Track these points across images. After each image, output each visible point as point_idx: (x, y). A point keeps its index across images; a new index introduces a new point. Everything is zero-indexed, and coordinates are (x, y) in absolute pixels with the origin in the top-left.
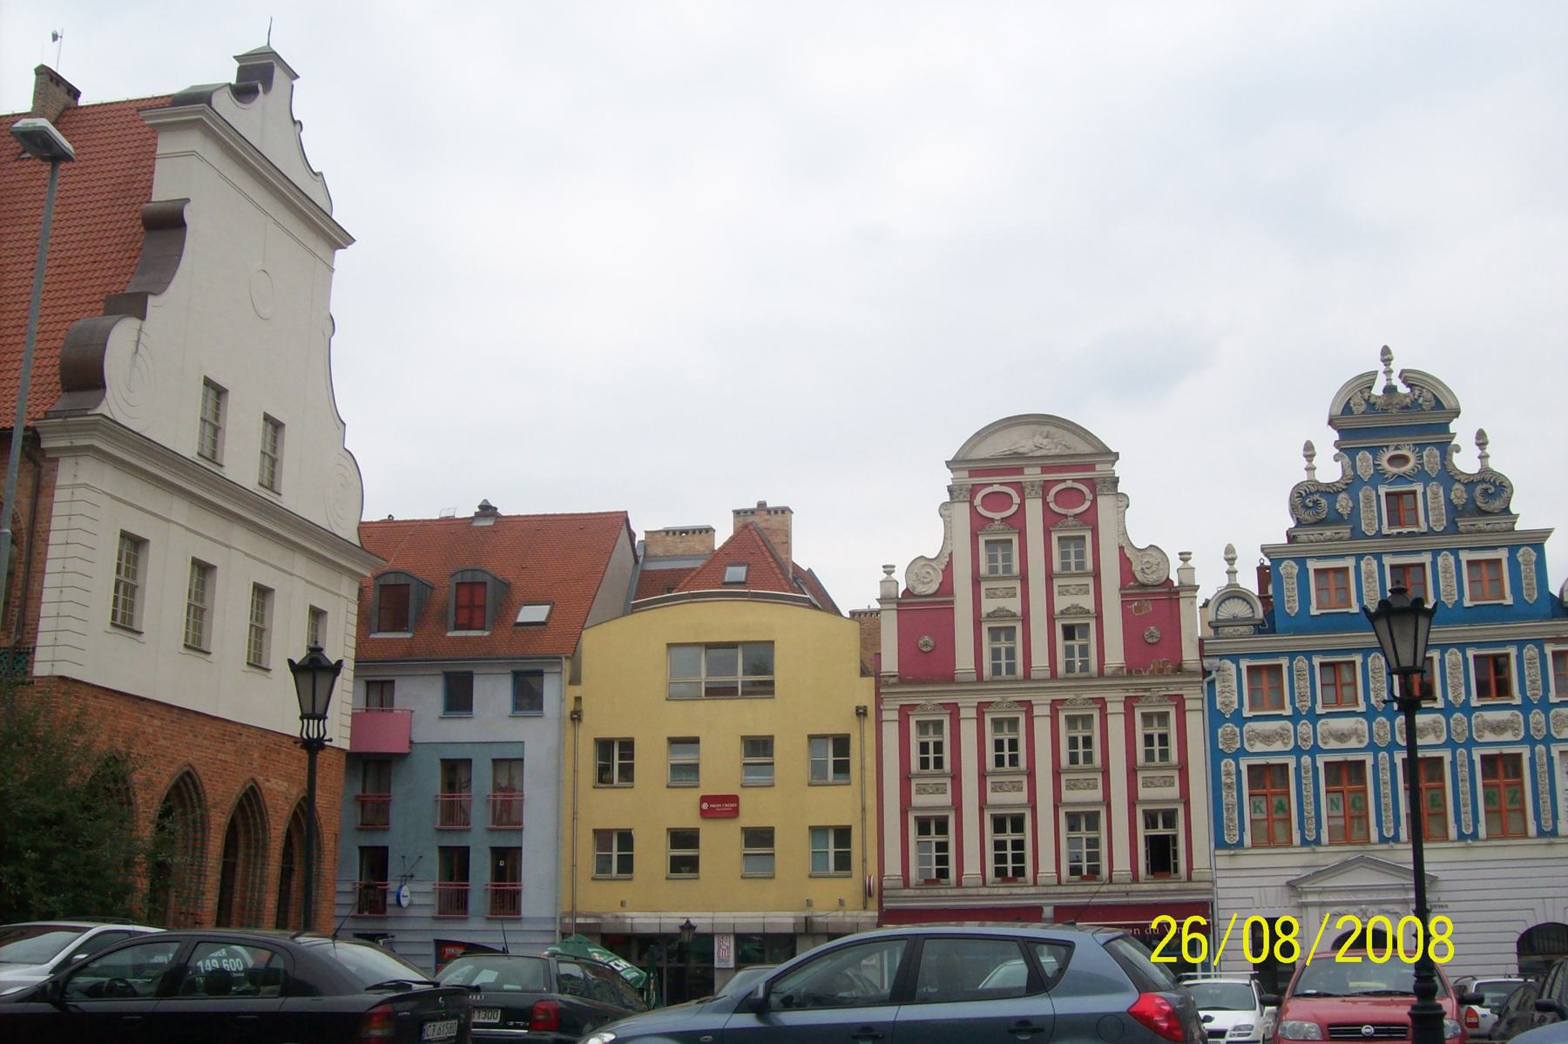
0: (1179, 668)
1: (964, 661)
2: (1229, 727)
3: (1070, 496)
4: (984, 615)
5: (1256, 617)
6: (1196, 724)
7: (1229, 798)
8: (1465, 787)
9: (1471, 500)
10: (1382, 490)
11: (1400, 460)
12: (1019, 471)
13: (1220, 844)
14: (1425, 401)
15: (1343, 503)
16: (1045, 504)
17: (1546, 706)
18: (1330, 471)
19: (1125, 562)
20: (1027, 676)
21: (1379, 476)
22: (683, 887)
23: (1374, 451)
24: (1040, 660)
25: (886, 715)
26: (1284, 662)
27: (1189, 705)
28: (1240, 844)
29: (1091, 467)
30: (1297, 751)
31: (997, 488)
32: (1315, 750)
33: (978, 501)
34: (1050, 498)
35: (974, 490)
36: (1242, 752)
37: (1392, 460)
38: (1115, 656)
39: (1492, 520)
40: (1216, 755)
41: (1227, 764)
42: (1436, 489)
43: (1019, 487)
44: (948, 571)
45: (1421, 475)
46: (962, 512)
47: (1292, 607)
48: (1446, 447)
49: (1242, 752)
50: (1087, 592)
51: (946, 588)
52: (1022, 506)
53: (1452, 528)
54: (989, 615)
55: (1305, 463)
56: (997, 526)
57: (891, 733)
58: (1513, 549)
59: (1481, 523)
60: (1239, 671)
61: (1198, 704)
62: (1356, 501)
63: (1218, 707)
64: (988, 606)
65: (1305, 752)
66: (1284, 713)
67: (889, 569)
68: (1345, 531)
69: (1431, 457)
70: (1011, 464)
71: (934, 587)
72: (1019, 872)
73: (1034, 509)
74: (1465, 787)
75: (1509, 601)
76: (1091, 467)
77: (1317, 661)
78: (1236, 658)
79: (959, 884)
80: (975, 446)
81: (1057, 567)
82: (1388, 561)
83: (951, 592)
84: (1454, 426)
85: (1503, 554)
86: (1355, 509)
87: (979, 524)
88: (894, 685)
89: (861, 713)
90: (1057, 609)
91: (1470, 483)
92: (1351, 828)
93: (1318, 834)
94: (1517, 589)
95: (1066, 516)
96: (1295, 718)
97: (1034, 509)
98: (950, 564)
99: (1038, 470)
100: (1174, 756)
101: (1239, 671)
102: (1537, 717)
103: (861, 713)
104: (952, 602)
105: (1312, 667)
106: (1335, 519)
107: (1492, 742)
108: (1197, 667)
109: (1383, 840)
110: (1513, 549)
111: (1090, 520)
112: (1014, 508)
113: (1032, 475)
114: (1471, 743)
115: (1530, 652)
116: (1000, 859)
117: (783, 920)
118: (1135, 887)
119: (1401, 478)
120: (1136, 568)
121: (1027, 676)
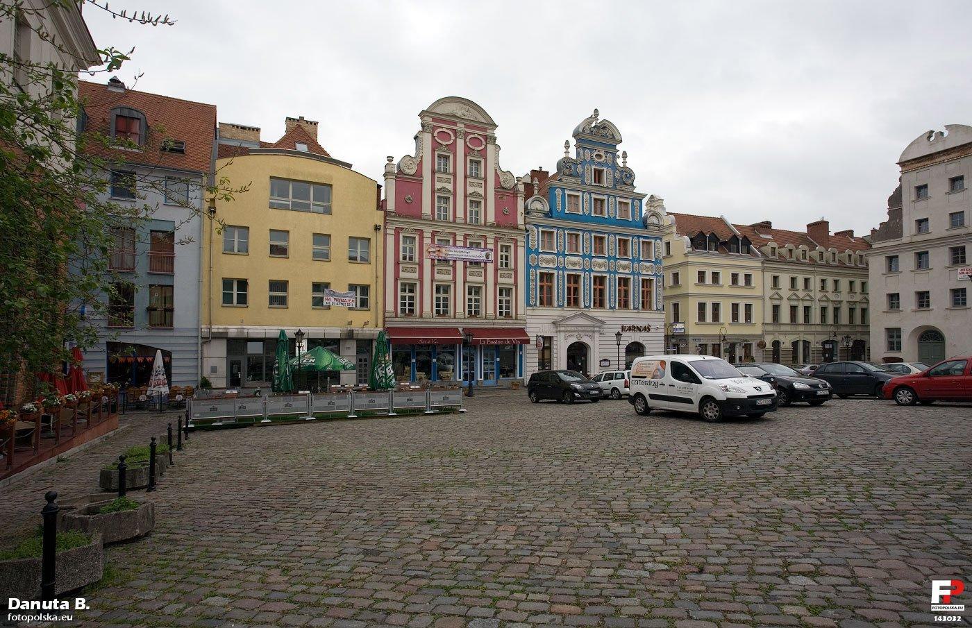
0: (516, 228)
1: (426, 209)
2: (532, 256)
4: (436, 189)
5: (545, 210)
6: (521, 252)
7: (532, 285)
8: (613, 289)
10: (593, 167)
11: (600, 156)
12: (455, 124)
13: (528, 305)
15: (579, 169)
16: (465, 142)
18: (573, 154)
19: (497, 175)
20: (454, 221)
22: (278, 312)
23: (592, 150)
24: (460, 214)
25: (388, 231)
26: (555, 231)
27: (519, 244)
28: (535, 305)
29: (485, 130)
30: (558, 268)
31: (444, 130)
32: (564, 269)
33: (435, 134)
34: (468, 140)
35: (435, 127)
36: (538, 266)
37: (596, 155)
38: (491, 218)
39: (628, 187)
40: (528, 267)
43: (455, 132)
44: (420, 164)
45: (605, 164)
46: (427, 138)
47: (559, 208)
48: (615, 156)
49: (538, 266)
50: (481, 187)
51: (419, 173)
52: (455, 141)
53: (614, 187)
54: (438, 190)
55: (565, 150)
56: (443, 148)
57: (391, 240)
59: (624, 187)
60: (538, 232)
61: (522, 244)
62: (584, 169)
63: (530, 246)
64: (438, 185)
65: (561, 269)
66: (554, 252)
67: (390, 159)
68: (580, 181)
70: (451, 119)
71: (412, 172)
72: (445, 312)
73: (460, 143)
74: (613, 289)
76: (485, 130)
77: (566, 232)
78: (537, 226)
79: (421, 316)
80: (434, 108)
81: (468, 174)
82: (593, 196)
83: (421, 176)
84: (618, 147)
86: (583, 172)
87: (436, 146)
88: (394, 216)
89: (377, 228)
90: (468, 193)
92: (573, 301)
93: (590, 304)
94: (633, 216)
95: (474, 150)
96: (558, 255)
97: (460, 143)
98: (421, 162)
99: (463, 126)
100: (512, 265)
101: (538, 232)
102: (636, 265)
103: (377, 228)
104: (422, 180)
105: (565, 234)
107: (623, 273)
108: (523, 227)
109: (585, 307)
111: (483, 153)
112: (452, 141)
113: (460, 127)
114: (616, 272)
115: (636, 240)
116: (403, 305)
117: (335, 332)
118: (496, 321)
119: (599, 163)
120: (501, 180)
121: (454, 221)
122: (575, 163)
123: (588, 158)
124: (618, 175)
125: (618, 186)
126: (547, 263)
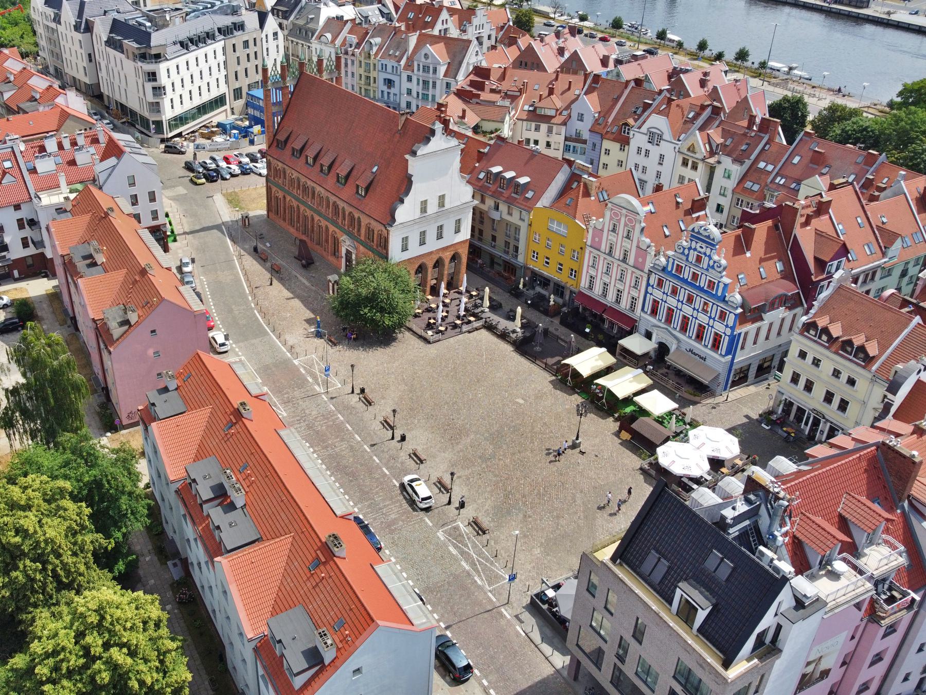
3: (630, 221)
9: (713, 266)
11: (701, 247)
14: (712, 238)
17: (714, 319)
21: (695, 249)
23: (697, 242)
36: (651, 294)
40: (646, 292)
41: (648, 295)
42: (707, 259)
47: (669, 269)
51: (602, 230)
53: (707, 270)
58: (719, 282)
69: (708, 250)
75: (714, 293)
85: (716, 282)
91: (715, 262)
103: (581, 248)
106: (683, 253)
110: (719, 282)
119: (700, 252)
122: (684, 249)
123: (693, 247)
124: (711, 263)
125: (710, 269)
126: (658, 294)
